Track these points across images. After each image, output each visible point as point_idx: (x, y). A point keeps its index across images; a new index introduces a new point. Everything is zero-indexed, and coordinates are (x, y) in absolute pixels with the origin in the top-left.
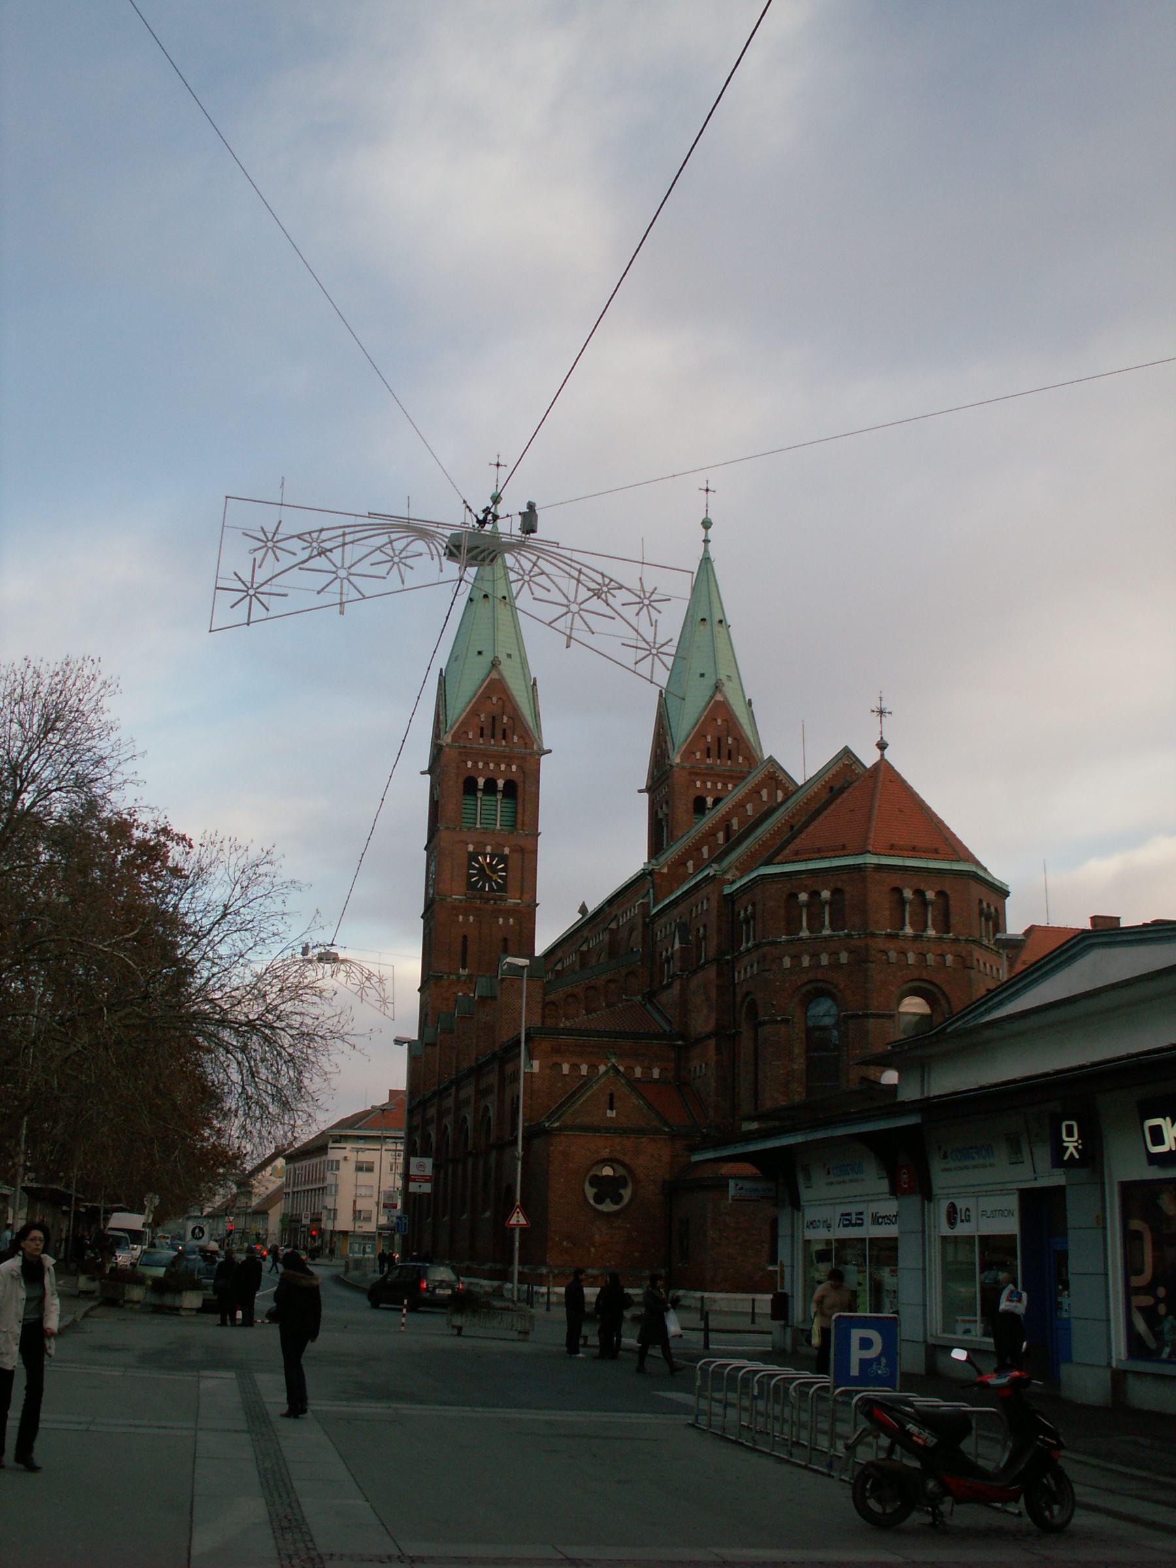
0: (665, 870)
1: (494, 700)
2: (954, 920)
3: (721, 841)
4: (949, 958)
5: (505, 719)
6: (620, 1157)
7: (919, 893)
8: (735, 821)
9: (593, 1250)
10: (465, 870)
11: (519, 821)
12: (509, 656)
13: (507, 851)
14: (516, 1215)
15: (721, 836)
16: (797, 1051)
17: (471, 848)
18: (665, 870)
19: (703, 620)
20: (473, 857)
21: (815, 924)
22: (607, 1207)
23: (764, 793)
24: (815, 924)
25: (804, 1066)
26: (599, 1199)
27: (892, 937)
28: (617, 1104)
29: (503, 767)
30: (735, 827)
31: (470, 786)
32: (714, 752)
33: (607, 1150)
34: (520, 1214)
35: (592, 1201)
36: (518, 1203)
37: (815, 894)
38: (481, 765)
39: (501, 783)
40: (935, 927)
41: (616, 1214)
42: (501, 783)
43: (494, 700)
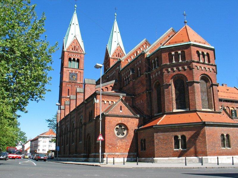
0: (123, 61)
1: (75, 43)
2: (211, 60)
3: (135, 55)
4: (211, 69)
5: (77, 47)
6: (124, 123)
7: (203, 53)
8: (138, 52)
9: (117, 148)
10: (68, 76)
11: (80, 67)
12: (78, 35)
13: (77, 72)
14: (100, 137)
15: (135, 54)
16: (173, 93)
17: (70, 71)
18: (123, 61)
19: (115, 32)
20: (70, 73)
21: (177, 59)
22: (120, 136)
23: (144, 46)
24: (177, 59)
25: (175, 97)
26: (118, 134)
27: (198, 62)
28: (122, 109)
29: (77, 56)
30: (138, 53)
31: (70, 60)
32: (118, 56)
33: (120, 121)
34: (101, 136)
35: (116, 135)
36: (100, 133)
37: (176, 53)
38: (72, 55)
39: (76, 59)
40: (207, 61)
41: (123, 138)
42: (76, 59)
43: (75, 43)
